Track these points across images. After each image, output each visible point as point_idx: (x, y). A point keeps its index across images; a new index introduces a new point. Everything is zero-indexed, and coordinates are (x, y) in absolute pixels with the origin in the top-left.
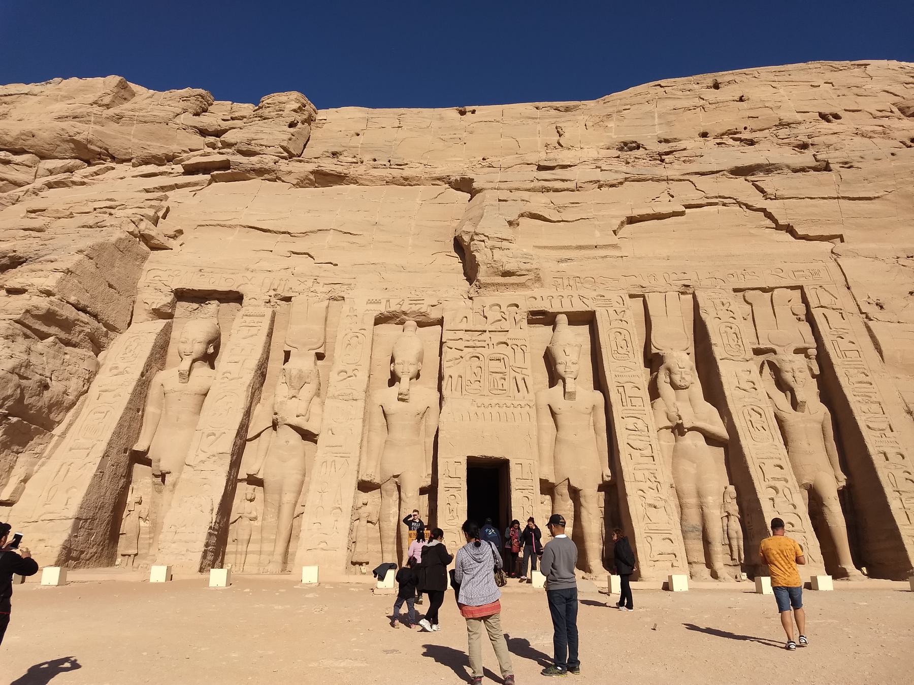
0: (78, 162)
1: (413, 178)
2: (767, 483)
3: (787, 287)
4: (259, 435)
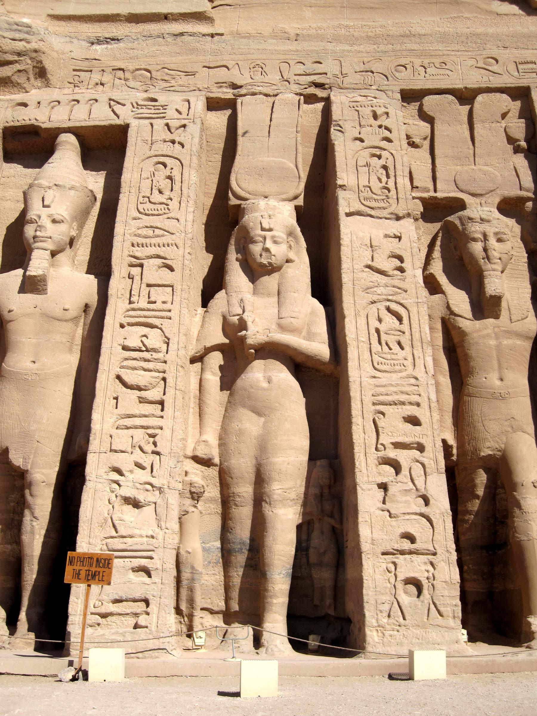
2: (380, 454)
3: (501, 90)
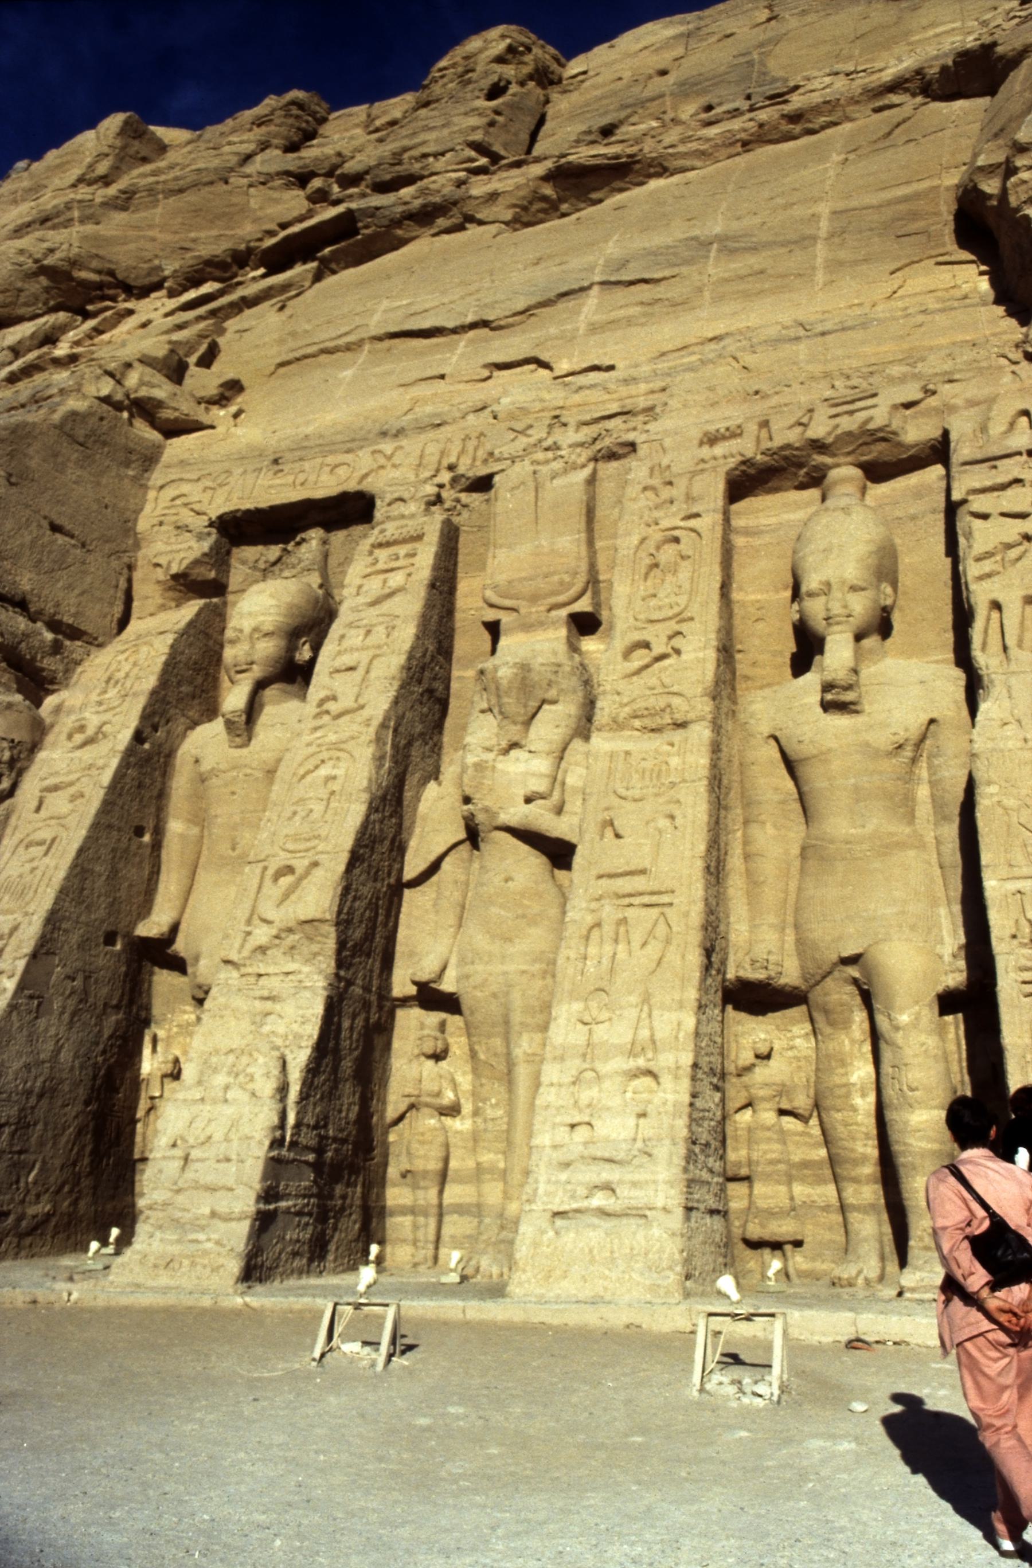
0: (62, 316)
1: (816, 110)
4: (434, 867)
